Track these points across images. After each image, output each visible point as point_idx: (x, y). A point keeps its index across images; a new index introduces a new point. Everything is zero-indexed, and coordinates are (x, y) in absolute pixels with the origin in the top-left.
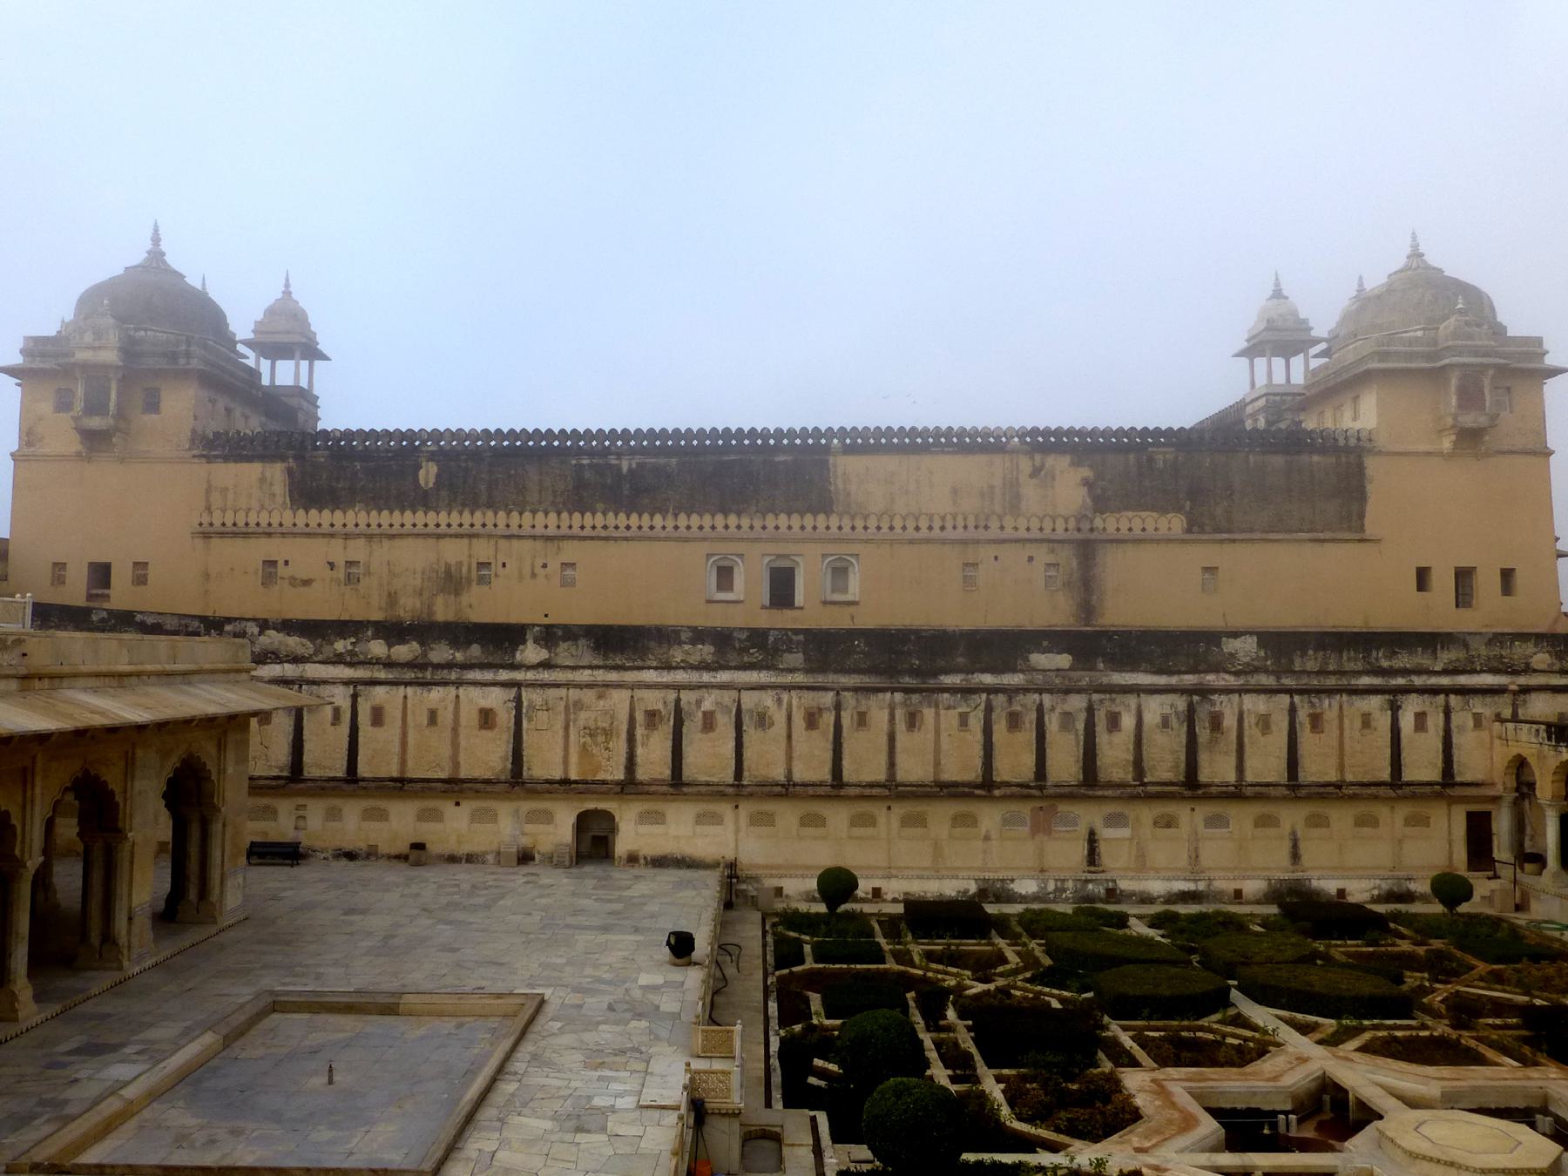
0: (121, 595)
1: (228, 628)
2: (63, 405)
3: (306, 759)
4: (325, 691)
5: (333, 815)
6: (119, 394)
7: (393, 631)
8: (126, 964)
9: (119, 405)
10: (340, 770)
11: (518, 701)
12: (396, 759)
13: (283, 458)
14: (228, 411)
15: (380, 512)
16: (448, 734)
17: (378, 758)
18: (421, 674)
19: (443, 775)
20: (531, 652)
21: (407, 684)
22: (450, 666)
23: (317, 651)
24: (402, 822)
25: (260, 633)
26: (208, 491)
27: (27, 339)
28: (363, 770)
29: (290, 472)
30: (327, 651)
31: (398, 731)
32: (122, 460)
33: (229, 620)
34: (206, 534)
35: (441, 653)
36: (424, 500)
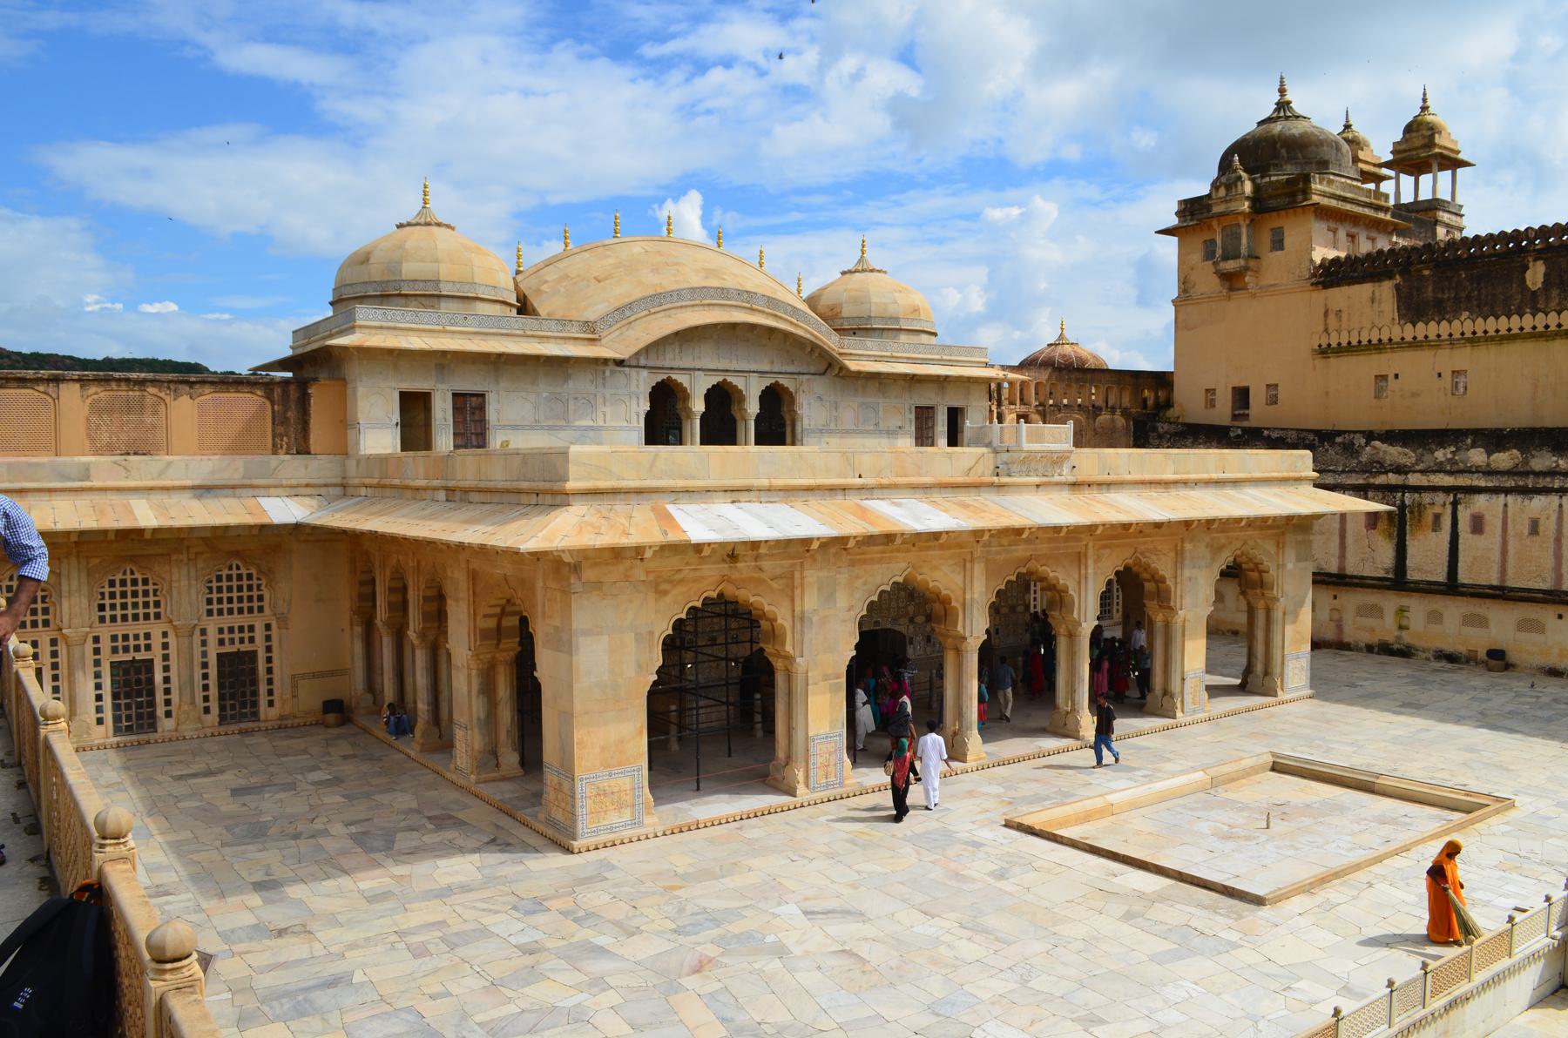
0: (1259, 414)
1: (1338, 440)
2: (1209, 255)
3: (1408, 563)
4: (1426, 498)
5: (1435, 617)
6: (1249, 236)
7: (1494, 439)
8: (1179, 714)
10: (1440, 575)
12: (1496, 568)
13: (1391, 277)
14: (1352, 237)
15: (1485, 319)
16: (1551, 545)
17: (1478, 566)
18: (1524, 485)
21: (1507, 491)
22: (1552, 473)
23: (1419, 460)
24: (1502, 626)
25: (1367, 444)
26: (1326, 314)
27: (1180, 202)
28: (1464, 577)
29: (1397, 287)
30: (1428, 461)
31: (1498, 539)
32: (1254, 296)
33: (1340, 433)
36: (1533, 302)
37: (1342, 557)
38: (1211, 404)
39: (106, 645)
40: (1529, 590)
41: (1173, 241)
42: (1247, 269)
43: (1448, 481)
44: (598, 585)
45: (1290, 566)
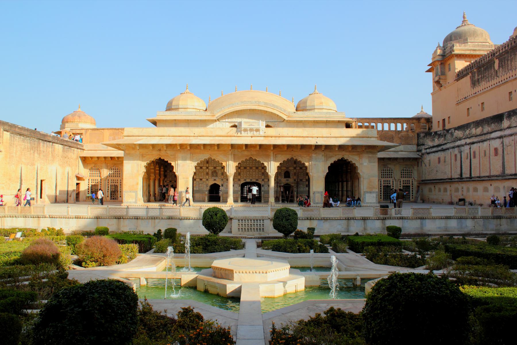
3: (463, 172)
6: (441, 68)
9: (441, 71)
11: (502, 143)
12: (478, 170)
16: (488, 159)
18: (483, 138)
19: (488, 174)
20: (506, 123)
21: (479, 142)
22: (488, 133)
28: (473, 176)
31: (478, 160)
33: (450, 129)
34: (458, 104)
35: (487, 129)
37: (451, 172)
38: (439, 127)
39: (110, 181)
40: (484, 177)
41: (431, 74)
42: (440, 79)
43: (468, 141)
44: (129, 154)
45: (365, 164)
